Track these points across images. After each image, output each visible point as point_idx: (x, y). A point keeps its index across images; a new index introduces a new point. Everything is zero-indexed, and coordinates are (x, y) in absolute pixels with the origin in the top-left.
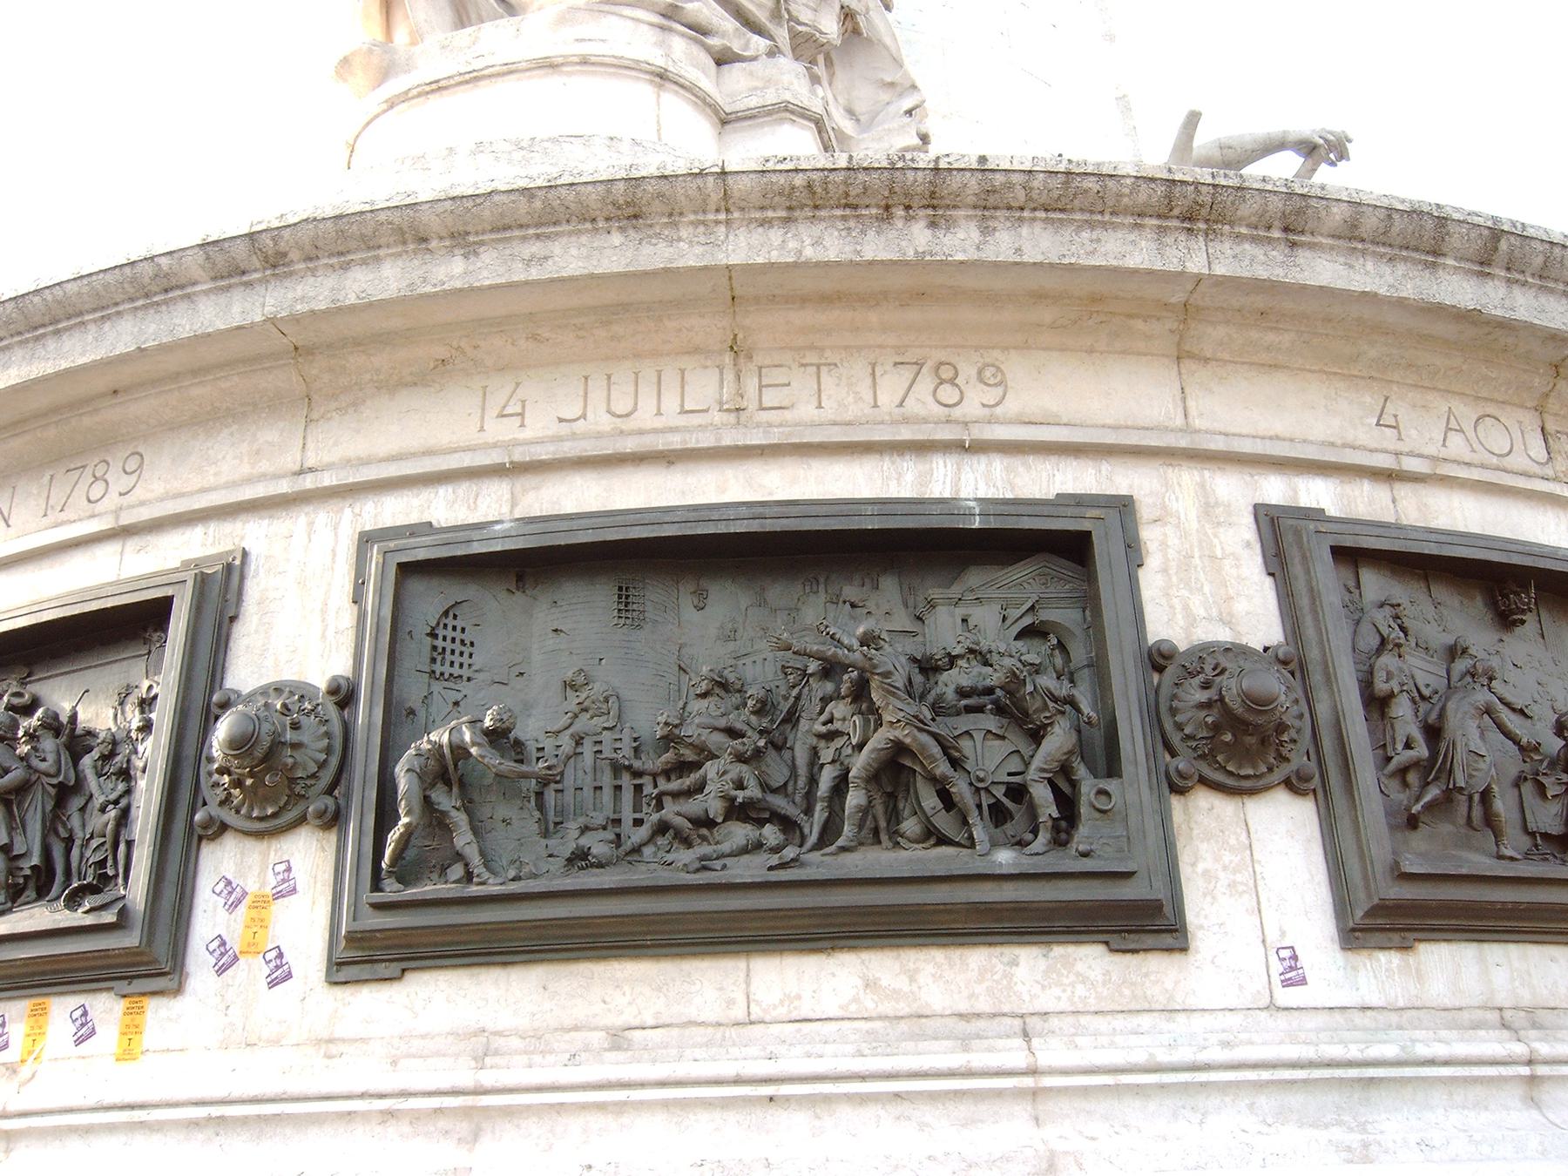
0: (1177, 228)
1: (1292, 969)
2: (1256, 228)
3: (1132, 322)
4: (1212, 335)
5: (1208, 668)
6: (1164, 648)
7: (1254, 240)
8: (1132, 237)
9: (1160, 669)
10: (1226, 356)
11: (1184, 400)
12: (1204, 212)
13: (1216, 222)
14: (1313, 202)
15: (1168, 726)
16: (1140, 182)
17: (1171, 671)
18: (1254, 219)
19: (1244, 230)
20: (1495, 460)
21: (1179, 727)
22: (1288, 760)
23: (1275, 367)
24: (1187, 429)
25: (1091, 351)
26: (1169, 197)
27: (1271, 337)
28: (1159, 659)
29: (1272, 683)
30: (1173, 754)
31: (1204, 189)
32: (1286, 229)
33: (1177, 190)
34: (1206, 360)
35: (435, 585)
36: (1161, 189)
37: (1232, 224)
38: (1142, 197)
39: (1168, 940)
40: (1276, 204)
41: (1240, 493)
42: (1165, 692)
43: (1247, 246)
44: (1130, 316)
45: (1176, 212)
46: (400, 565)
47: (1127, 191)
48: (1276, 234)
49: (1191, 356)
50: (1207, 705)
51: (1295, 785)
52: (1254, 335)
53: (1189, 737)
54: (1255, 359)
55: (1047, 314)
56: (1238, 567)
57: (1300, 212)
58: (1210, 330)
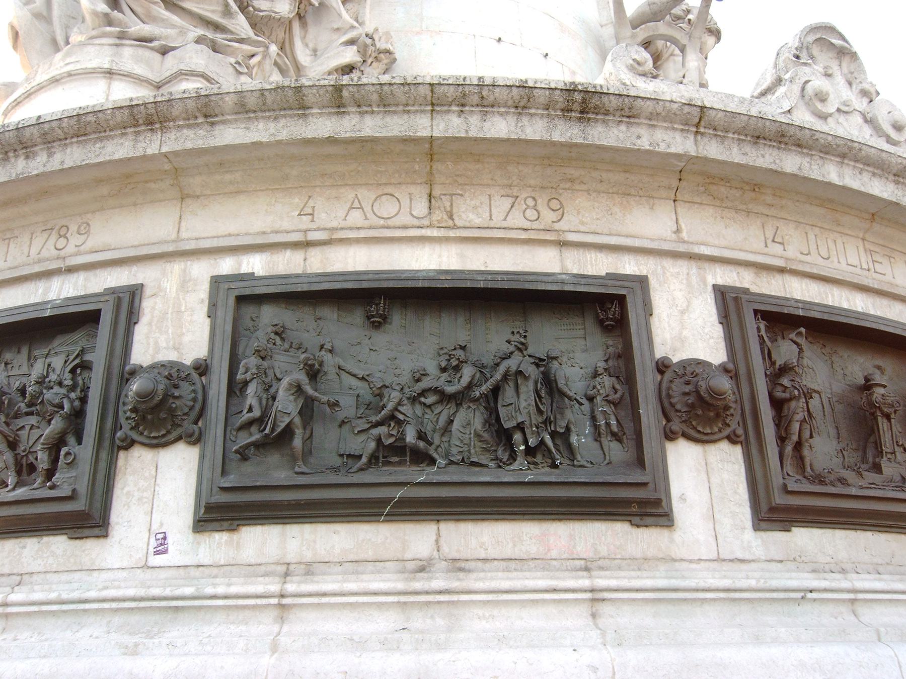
0: (144, 131)
1: (161, 544)
2: (189, 119)
3: (148, 185)
4: (195, 182)
7: (189, 126)
8: (122, 141)
10: (208, 192)
11: (180, 222)
12: (155, 118)
13: (166, 121)
14: (213, 98)
16: (115, 111)
18: (184, 115)
19: (181, 123)
20: (382, 222)
23: (238, 192)
24: (178, 240)
25: (135, 205)
26: (132, 114)
27: (228, 177)
31: (149, 106)
32: (206, 116)
33: (135, 110)
34: (198, 197)
36: (126, 112)
37: (174, 120)
38: (119, 119)
40: (191, 104)
41: (202, 271)
43: (185, 131)
44: (146, 182)
45: (141, 122)
47: (109, 117)
48: (200, 120)
49: (188, 196)
52: (218, 177)
54: (226, 191)
55: (104, 190)
56: (192, 315)
57: (206, 105)
58: (191, 180)
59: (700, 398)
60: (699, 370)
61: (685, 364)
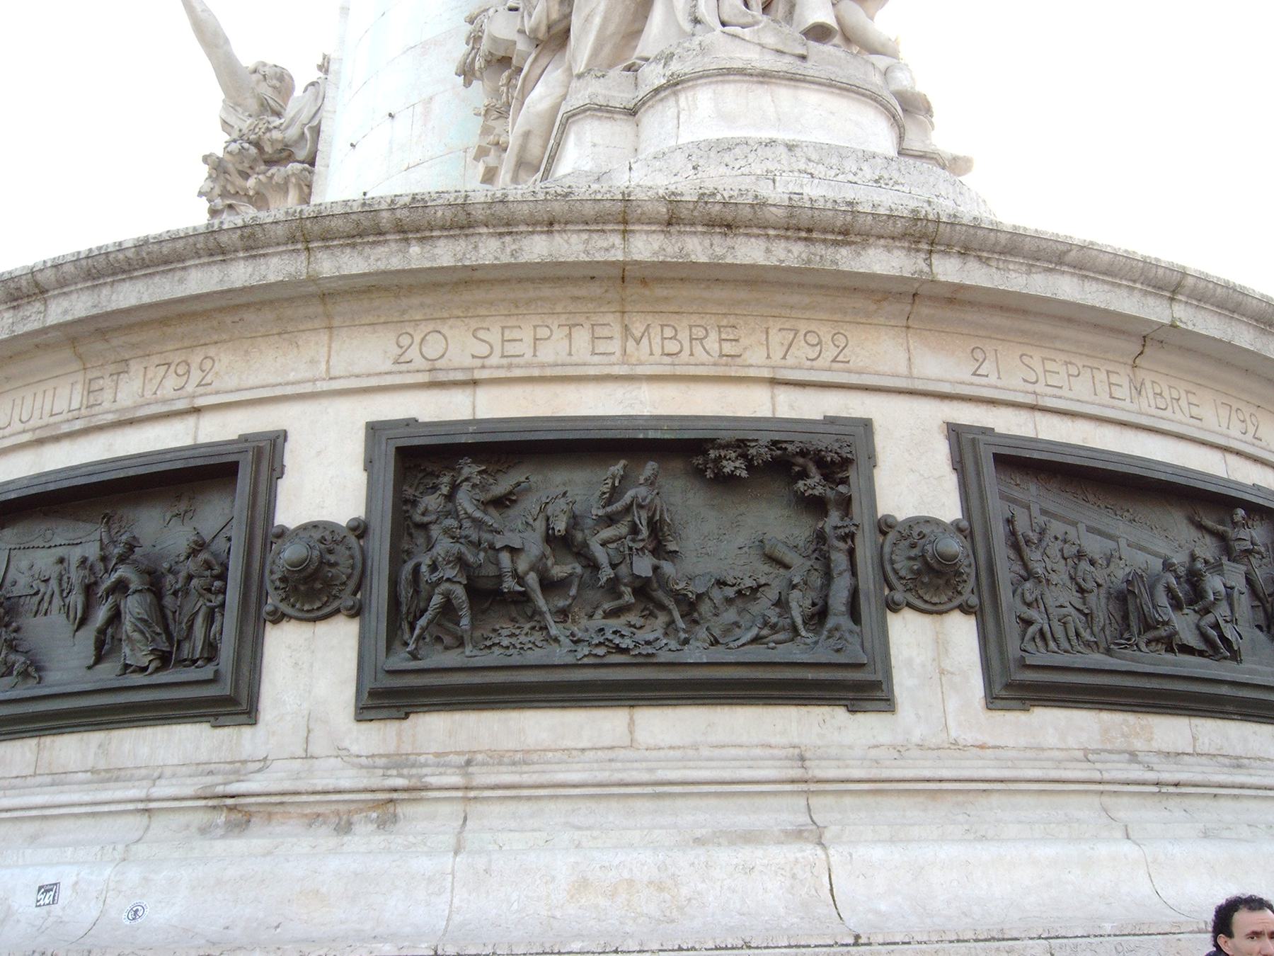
5: (915, 534)
6: (889, 520)
9: (884, 533)
15: (888, 568)
17: (892, 536)
21: (896, 572)
22: (960, 593)
28: (885, 526)
29: (953, 545)
30: (891, 588)
35: (416, 462)
39: (882, 705)
42: (887, 549)
46: (398, 449)
50: (910, 558)
51: (966, 609)
53: (901, 578)
59: (926, 563)
60: (926, 530)
61: (913, 522)
